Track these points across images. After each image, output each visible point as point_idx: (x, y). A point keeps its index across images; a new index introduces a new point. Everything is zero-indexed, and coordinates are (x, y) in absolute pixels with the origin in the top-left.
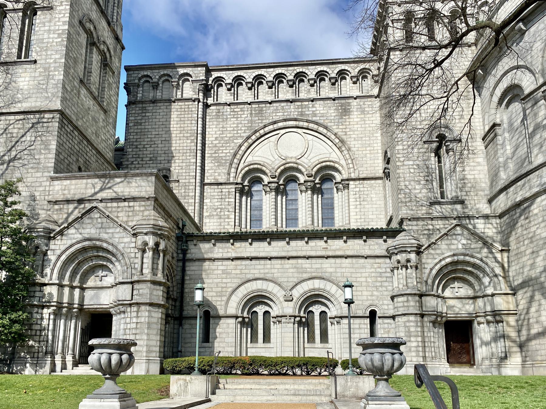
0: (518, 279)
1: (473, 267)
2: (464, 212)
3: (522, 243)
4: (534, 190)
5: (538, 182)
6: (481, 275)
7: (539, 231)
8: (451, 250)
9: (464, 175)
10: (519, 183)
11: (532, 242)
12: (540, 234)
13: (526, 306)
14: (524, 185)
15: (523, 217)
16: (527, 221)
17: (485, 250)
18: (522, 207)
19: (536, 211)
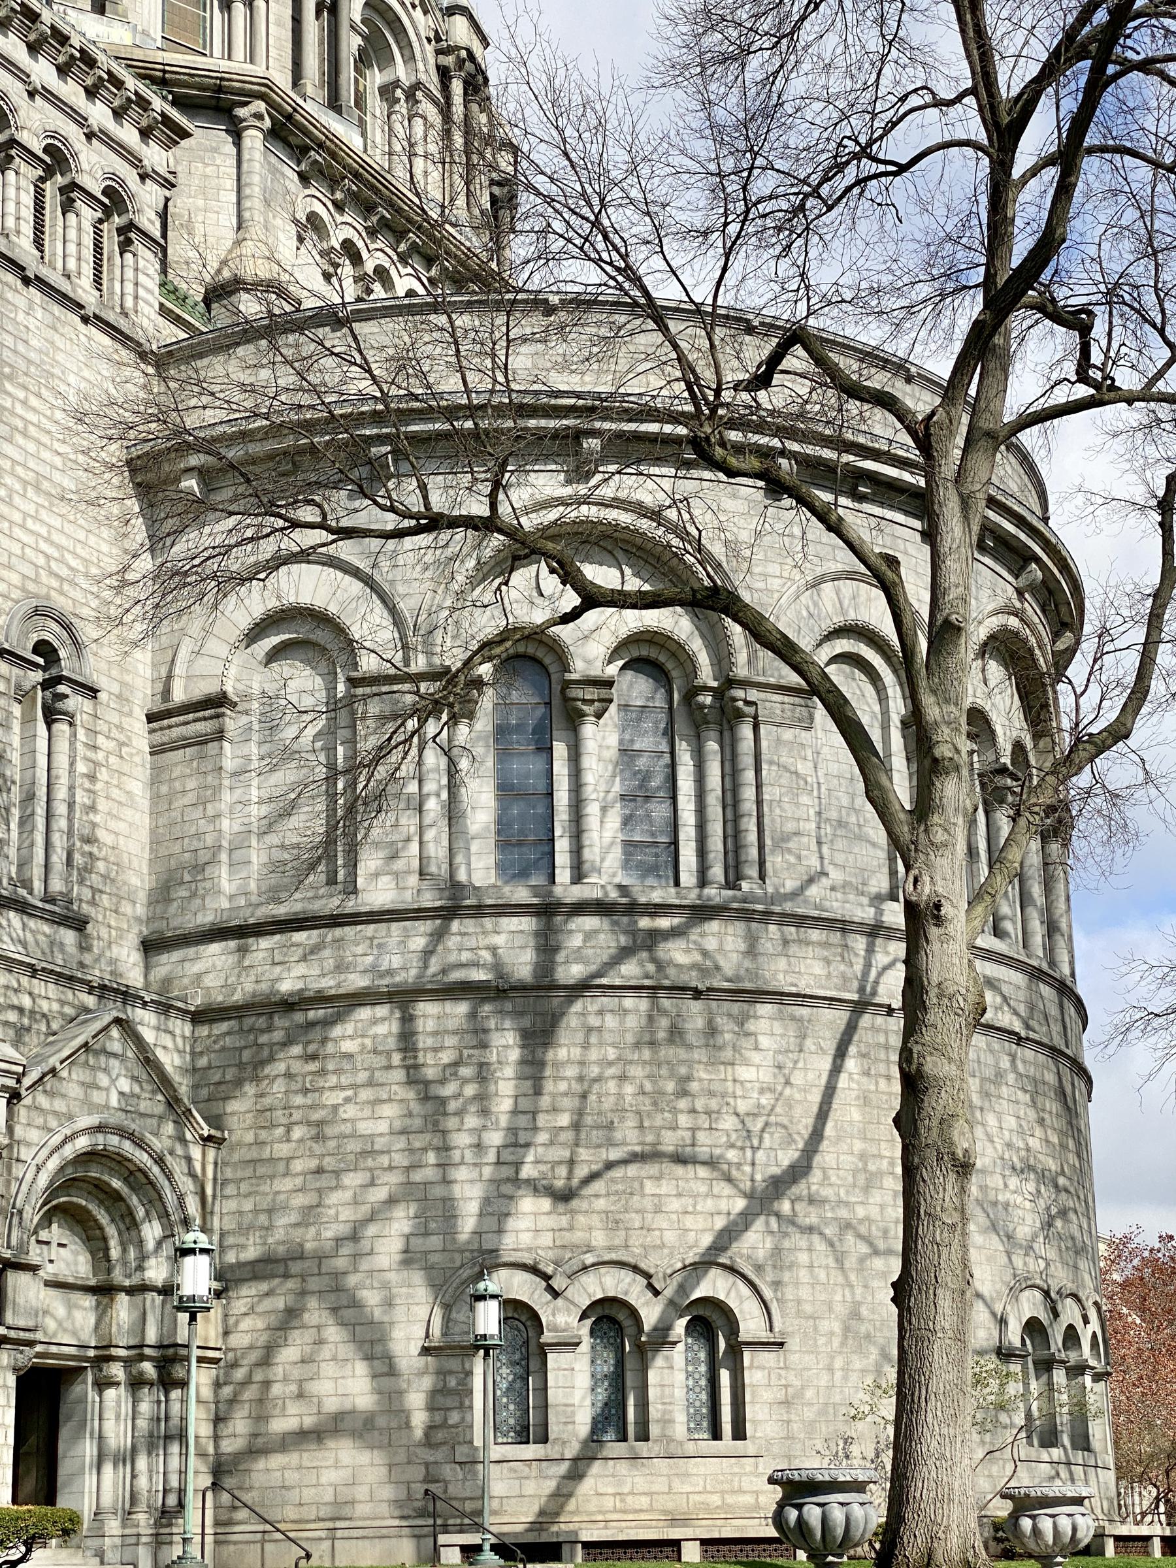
0: (243, 1247)
1: (126, 1180)
2: (82, 965)
3: (280, 1131)
4: (352, 976)
5: (369, 960)
6: (141, 1212)
7: (349, 1112)
8: (92, 1108)
9: (94, 825)
10: (299, 937)
11: (319, 1137)
12: (353, 1121)
13: (263, 1339)
14: (316, 949)
15: (296, 1050)
16: (313, 1066)
17: (169, 1128)
18: (299, 1017)
19: (348, 1046)
